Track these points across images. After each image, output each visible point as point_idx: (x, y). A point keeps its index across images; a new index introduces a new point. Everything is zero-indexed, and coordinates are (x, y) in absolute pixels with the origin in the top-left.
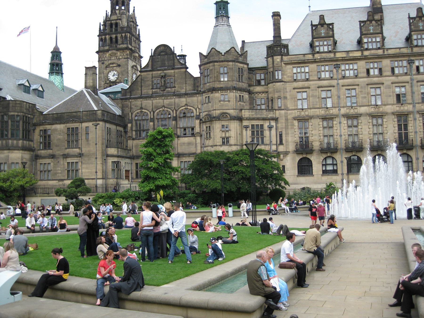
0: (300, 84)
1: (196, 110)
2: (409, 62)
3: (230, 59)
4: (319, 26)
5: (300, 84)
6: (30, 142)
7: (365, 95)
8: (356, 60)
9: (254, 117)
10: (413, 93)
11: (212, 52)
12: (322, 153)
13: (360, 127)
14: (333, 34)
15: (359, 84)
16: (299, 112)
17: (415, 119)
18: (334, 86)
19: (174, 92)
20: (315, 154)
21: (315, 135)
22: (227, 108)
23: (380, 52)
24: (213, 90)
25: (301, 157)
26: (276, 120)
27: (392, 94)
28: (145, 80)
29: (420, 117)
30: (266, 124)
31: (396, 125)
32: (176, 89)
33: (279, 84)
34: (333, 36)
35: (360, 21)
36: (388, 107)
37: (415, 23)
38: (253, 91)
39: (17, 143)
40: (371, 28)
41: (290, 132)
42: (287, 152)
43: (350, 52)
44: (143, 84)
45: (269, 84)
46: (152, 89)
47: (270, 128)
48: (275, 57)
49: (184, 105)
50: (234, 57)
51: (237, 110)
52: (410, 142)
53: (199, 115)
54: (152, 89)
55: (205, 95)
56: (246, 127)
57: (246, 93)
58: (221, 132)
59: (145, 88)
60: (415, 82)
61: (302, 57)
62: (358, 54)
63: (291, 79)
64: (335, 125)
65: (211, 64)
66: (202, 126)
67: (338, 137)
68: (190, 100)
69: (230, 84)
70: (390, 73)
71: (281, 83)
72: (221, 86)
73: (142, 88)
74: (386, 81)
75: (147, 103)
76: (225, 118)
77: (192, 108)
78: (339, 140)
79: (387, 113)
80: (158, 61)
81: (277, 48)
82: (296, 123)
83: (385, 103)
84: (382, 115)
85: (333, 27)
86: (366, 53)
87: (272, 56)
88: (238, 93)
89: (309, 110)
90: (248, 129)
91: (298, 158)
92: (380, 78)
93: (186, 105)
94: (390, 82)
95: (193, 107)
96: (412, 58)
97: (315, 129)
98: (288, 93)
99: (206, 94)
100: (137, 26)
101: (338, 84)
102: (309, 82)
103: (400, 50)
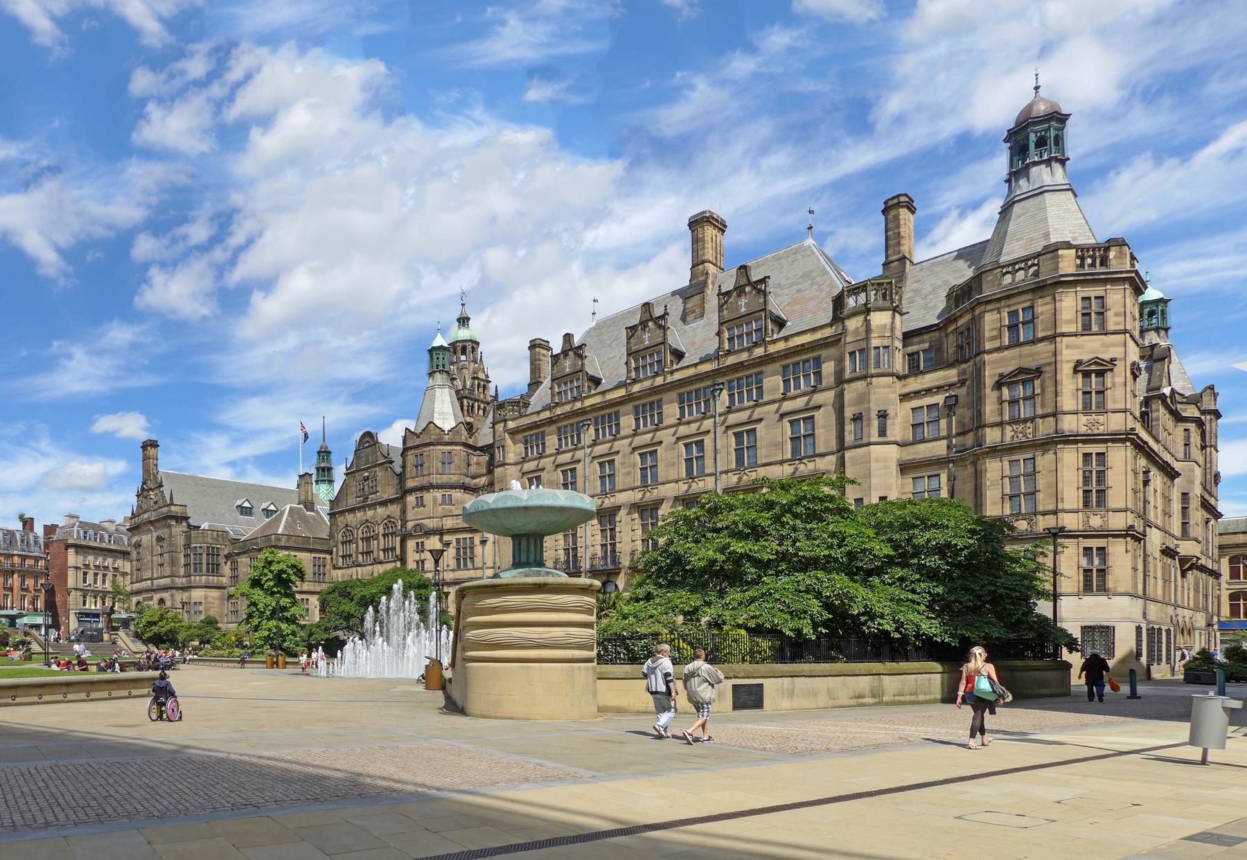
6: (220, 578)
39: (200, 580)
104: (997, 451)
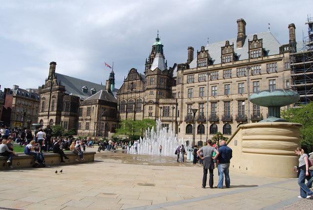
24: (148, 89)
30: (172, 106)
36: (233, 96)
47: (174, 108)
56: (161, 108)
70: (235, 76)
75: (125, 96)
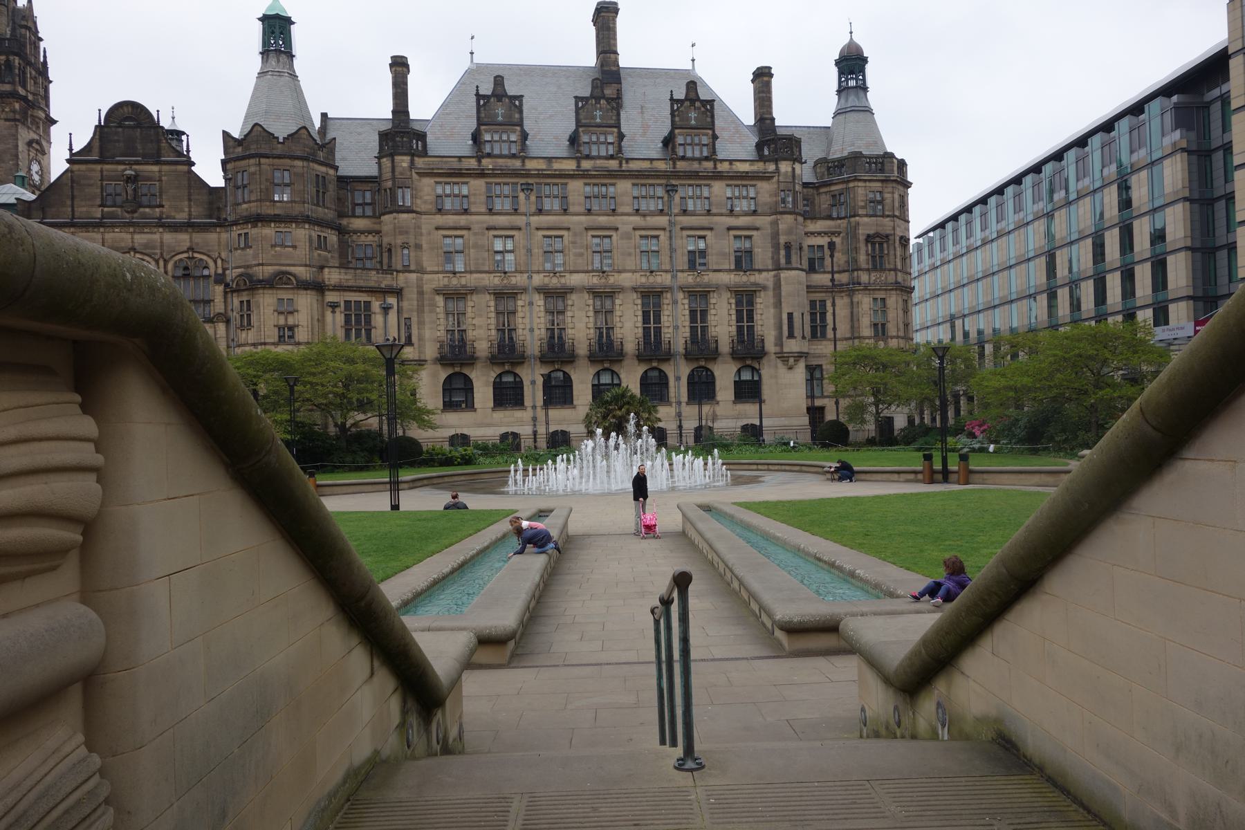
0: (451, 220)
1: (215, 262)
2: (669, 188)
3: (299, 153)
4: (492, 100)
5: (451, 220)
7: (582, 250)
8: (565, 178)
9: (350, 284)
10: (672, 250)
11: (253, 134)
12: (493, 364)
13: (569, 314)
14: (521, 119)
15: (571, 226)
16: (446, 279)
17: (675, 302)
18: (520, 229)
19: (160, 218)
20: (479, 365)
21: (480, 327)
22: (292, 262)
23: (613, 164)
24: (258, 220)
25: (450, 371)
26: (398, 293)
27: (633, 251)
28: (82, 182)
29: (685, 298)
31: (640, 313)
32: (164, 210)
33: (405, 216)
34: (520, 124)
35: (576, 97)
36: (624, 275)
37: (682, 111)
38: (348, 226)
40: (598, 113)
41: (427, 317)
42: (420, 361)
43: (554, 160)
44: (76, 193)
45: (384, 214)
46: (100, 206)
47: (386, 309)
48: (398, 158)
49: (185, 249)
50: (307, 149)
51: (313, 266)
52: (664, 346)
53: (224, 274)
54: (102, 205)
55: (236, 231)
56: (334, 306)
57: (333, 232)
58: (276, 314)
59: (83, 203)
60: (678, 227)
61: (455, 164)
62: (570, 165)
63: (431, 207)
64: (520, 309)
65: (252, 161)
66: (229, 300)
67: (527, 332)
68: (199, 237)
69: (297, 209)
71: (411, 215)
72: (277, 212)
73: (75, 203)
74: (623, 224)
76: (286, 284)
77: (204, 257)
78: (528, 338)
79: (622, 289)
80: (118, 141)
81: (402, 137)
82: (440, 300)
83: (620, 268)
84: (614, 292)
85: (521, 104)
86: (586, 164)
87: (392, 155)
88: (315, 232)
89: (468, 276)
90: (337, 310)
91: (443, 375)
92: (611, 218)
93: (191, 249)
94: (631, 226)
95: (209, 256)
96: (674, 182)
97: (481, 316)
98: (424, 238)
99: (239, 227)
100: (41, 40)
101: (528, 224)
102: (469, 217)
103: (651, 163)
104: (867, 289)
